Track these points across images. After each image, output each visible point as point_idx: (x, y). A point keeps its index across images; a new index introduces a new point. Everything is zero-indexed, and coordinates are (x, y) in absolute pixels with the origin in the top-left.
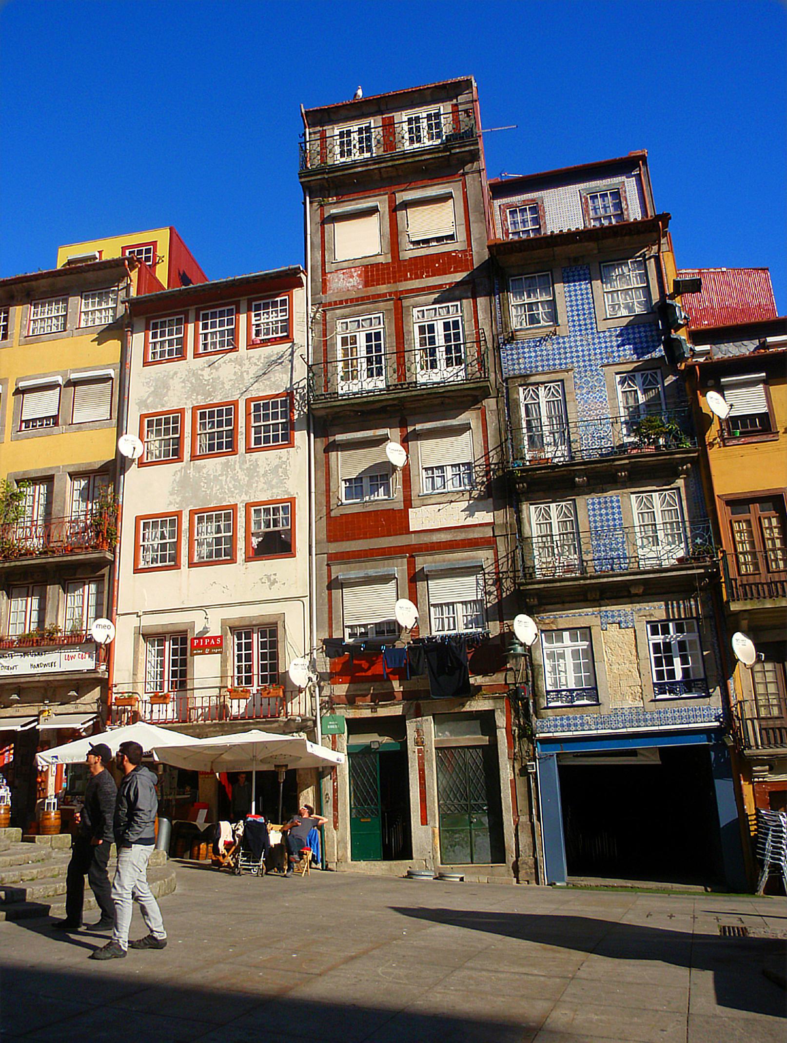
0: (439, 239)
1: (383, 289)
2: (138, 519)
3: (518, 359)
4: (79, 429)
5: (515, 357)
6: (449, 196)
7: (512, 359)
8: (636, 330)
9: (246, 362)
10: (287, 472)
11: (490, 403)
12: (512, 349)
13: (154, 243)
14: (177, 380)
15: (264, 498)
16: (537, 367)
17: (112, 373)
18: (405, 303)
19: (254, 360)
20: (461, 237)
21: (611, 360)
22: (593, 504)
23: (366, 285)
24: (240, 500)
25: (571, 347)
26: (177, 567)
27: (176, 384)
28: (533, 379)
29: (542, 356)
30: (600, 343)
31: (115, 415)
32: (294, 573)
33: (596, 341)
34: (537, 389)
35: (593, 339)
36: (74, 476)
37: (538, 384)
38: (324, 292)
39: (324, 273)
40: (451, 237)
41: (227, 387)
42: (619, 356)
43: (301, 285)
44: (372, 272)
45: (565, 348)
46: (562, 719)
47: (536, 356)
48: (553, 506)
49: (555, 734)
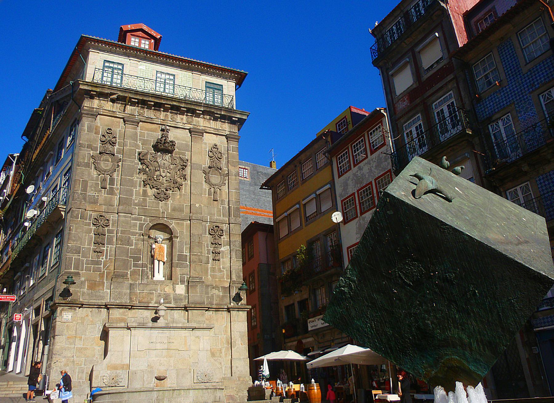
0: (437, 62)
1: (418, 101)
2: (348, 248)
3: (485, 110)
4: (324, 214)
5: (483, 109)
7: (482, 111)
8: (545, 63)
9: (371, 162)
12: (480, 106)
14: (350, 180)
16: (495, 110)
19: (374, 160)
21: (534, 88)
22: (540, 180)
23: (411, 100)
25: (510, 91)
27: (350, 182)
28: (494, 118)
29: (496, 102)
30: (526, 81)
31: (334, 203)
33: (524, 80)
34: (498, 122)
35: (521, 80)
37: (497, 119)
38: (395, 113)
39: (394, 105)
40: (441, 59)
41: (367, 176)
42: (538, 84)
45: (507, 92)
46: (547, 318)
47: (493, 104)
48: (518, 188)
49: (545, 328)
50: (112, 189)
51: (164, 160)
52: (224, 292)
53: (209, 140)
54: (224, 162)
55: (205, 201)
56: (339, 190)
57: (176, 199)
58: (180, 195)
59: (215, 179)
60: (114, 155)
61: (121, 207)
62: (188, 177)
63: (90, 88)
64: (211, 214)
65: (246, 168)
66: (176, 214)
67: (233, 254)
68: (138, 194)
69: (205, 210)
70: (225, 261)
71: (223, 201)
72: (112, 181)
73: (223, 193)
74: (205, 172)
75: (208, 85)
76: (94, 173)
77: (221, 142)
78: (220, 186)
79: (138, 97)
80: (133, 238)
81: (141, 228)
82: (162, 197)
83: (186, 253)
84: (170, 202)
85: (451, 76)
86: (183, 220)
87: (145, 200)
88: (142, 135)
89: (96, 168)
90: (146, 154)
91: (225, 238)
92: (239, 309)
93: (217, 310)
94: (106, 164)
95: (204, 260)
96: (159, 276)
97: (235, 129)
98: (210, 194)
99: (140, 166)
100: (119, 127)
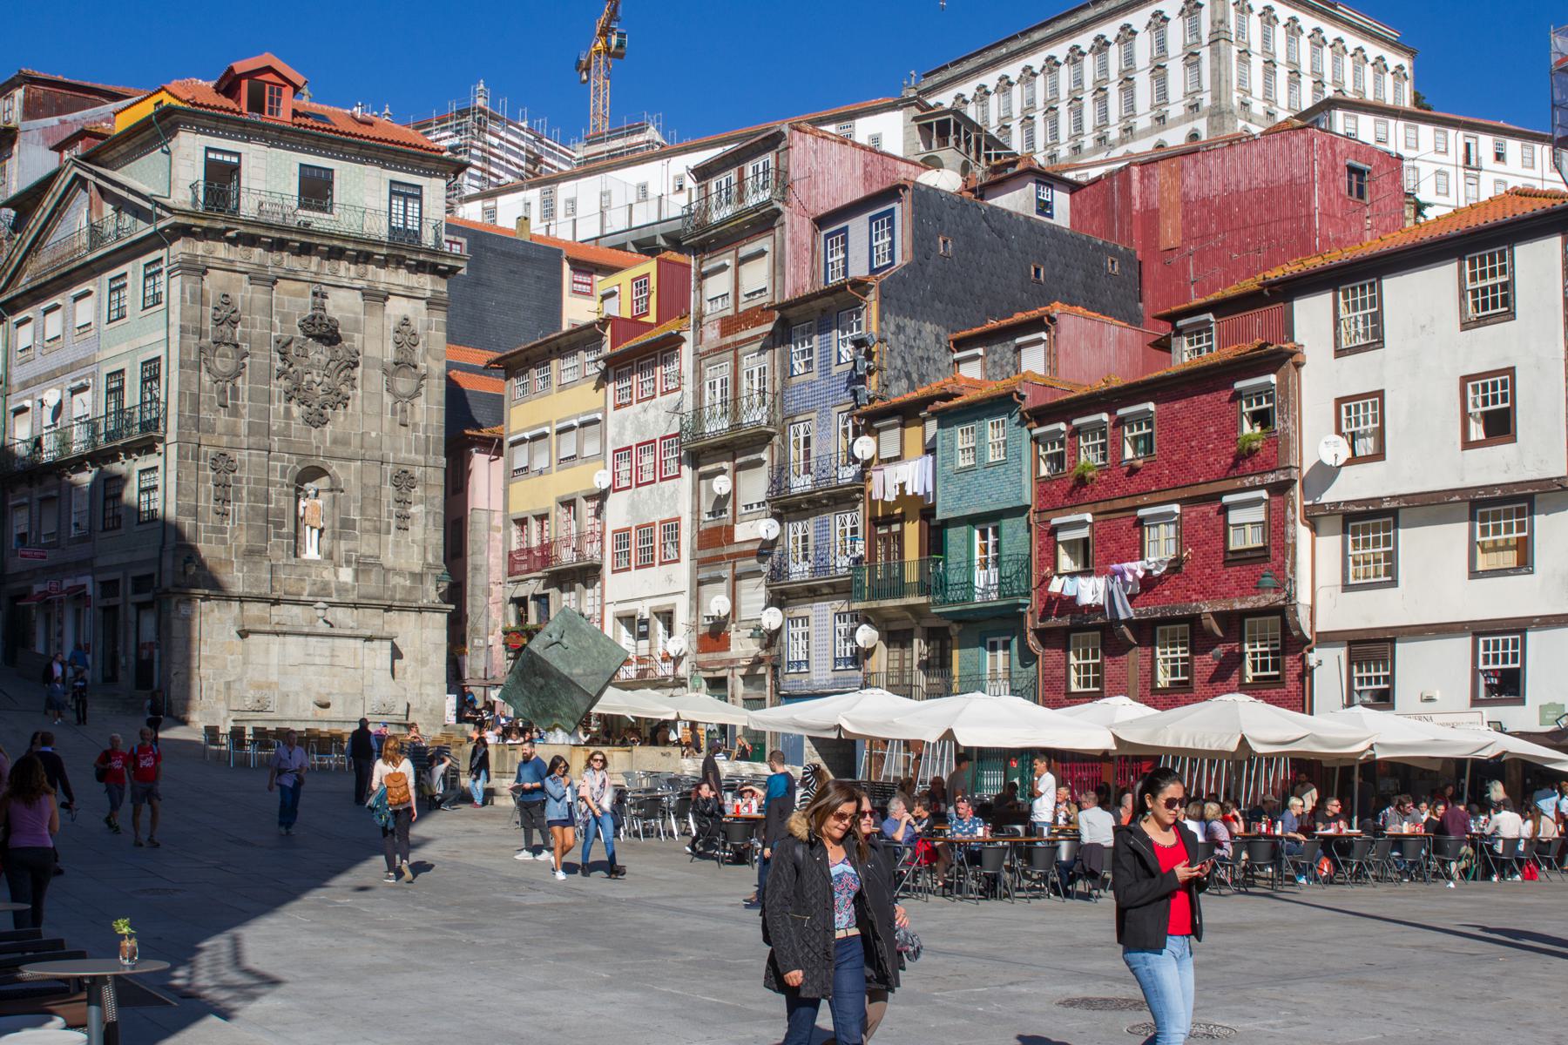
0: (760, 291)
1: (729, 339)
6: (761, 253)
10: (677, 498)
11: (776, 439)
13: (648, 275)
15: (667, 517)
17: (599, 416)
18: (740, 352)
20: (769, 291)
24: (656, 518)
26: (628, 569)
27: (628, 424)
32: (682, 573)
36: (587, 498)
43: (683, 340)
44: (729, 325)
50: (235, 406)
51: (319, 354)
52: (414, 581)
53: (397, 308)
54: (419, 349)
55: (386, 427)
56: (612, 431)
57: (339, 422)
58: (345, 415)
59: (404, 384)
60: (237, 346)
61: (252, 440)
62: (358, 382)
63: (192, 221)
64: (396, 450)
65: (459, 239)
66: (339, 451)
67: (431, 520)
68: (277, 416)
69: (386, 441)
70: (416, 531)
71: (415, 425)
72: (235, 391)
73: (417, 410)
74: (385, 372)
75: (396, 189)
76: (206, 379)
77: (414, 311)
78: (411, 397)
79: (274, 234)
80: (272, 490)
81: (283, 475)
82: (317, 420)
83: (355, 515)
84: (328, 428)
85: (769, 327)
86: (350, 459)
87: (288, 425)
88: (281, 304)
89: (209, 371)
90: (289, 343)
91: (418, 491)
92: (435, 610)
93: (401, 609)
94: (223, 364)
95: (384, 527)
96: (311, 552)
97: (442, 286)
98: (394, 413)
99: (279, 364)
100: (244, 292)
